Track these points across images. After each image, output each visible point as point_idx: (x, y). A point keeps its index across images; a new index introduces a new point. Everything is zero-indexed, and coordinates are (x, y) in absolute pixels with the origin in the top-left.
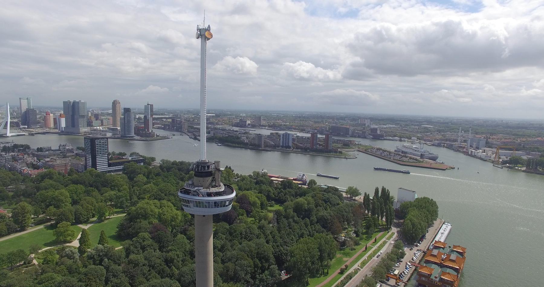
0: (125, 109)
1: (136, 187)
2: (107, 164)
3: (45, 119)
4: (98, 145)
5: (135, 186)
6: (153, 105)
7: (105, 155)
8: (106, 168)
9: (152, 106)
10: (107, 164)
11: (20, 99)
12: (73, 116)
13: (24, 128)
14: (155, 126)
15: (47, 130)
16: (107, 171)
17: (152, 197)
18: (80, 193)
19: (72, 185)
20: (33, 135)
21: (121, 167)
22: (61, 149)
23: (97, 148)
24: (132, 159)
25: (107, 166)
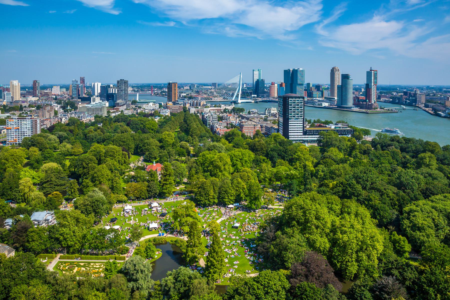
1: (322, 166)
2: (302, 131)
4: (291, 105)
5: (322, 164)
8: (300, 136)
11: (253, 70)
13: (254, 97)
14: (382, 99)
15: (271, 99)
16: (301, 140)
17: (340, 186)
18: (246, 162)
20: (257, 102)
21: (315, 138)
23: (291, 110)
25: (302, 134)
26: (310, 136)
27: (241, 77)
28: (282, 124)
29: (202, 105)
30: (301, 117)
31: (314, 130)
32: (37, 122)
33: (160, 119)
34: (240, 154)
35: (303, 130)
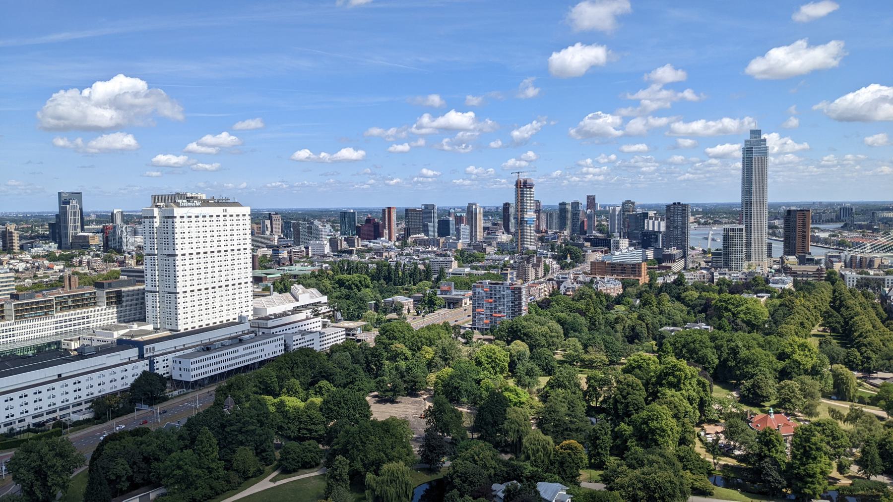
29: (876, 266)
32: (521, 293)
33: (771, 298)
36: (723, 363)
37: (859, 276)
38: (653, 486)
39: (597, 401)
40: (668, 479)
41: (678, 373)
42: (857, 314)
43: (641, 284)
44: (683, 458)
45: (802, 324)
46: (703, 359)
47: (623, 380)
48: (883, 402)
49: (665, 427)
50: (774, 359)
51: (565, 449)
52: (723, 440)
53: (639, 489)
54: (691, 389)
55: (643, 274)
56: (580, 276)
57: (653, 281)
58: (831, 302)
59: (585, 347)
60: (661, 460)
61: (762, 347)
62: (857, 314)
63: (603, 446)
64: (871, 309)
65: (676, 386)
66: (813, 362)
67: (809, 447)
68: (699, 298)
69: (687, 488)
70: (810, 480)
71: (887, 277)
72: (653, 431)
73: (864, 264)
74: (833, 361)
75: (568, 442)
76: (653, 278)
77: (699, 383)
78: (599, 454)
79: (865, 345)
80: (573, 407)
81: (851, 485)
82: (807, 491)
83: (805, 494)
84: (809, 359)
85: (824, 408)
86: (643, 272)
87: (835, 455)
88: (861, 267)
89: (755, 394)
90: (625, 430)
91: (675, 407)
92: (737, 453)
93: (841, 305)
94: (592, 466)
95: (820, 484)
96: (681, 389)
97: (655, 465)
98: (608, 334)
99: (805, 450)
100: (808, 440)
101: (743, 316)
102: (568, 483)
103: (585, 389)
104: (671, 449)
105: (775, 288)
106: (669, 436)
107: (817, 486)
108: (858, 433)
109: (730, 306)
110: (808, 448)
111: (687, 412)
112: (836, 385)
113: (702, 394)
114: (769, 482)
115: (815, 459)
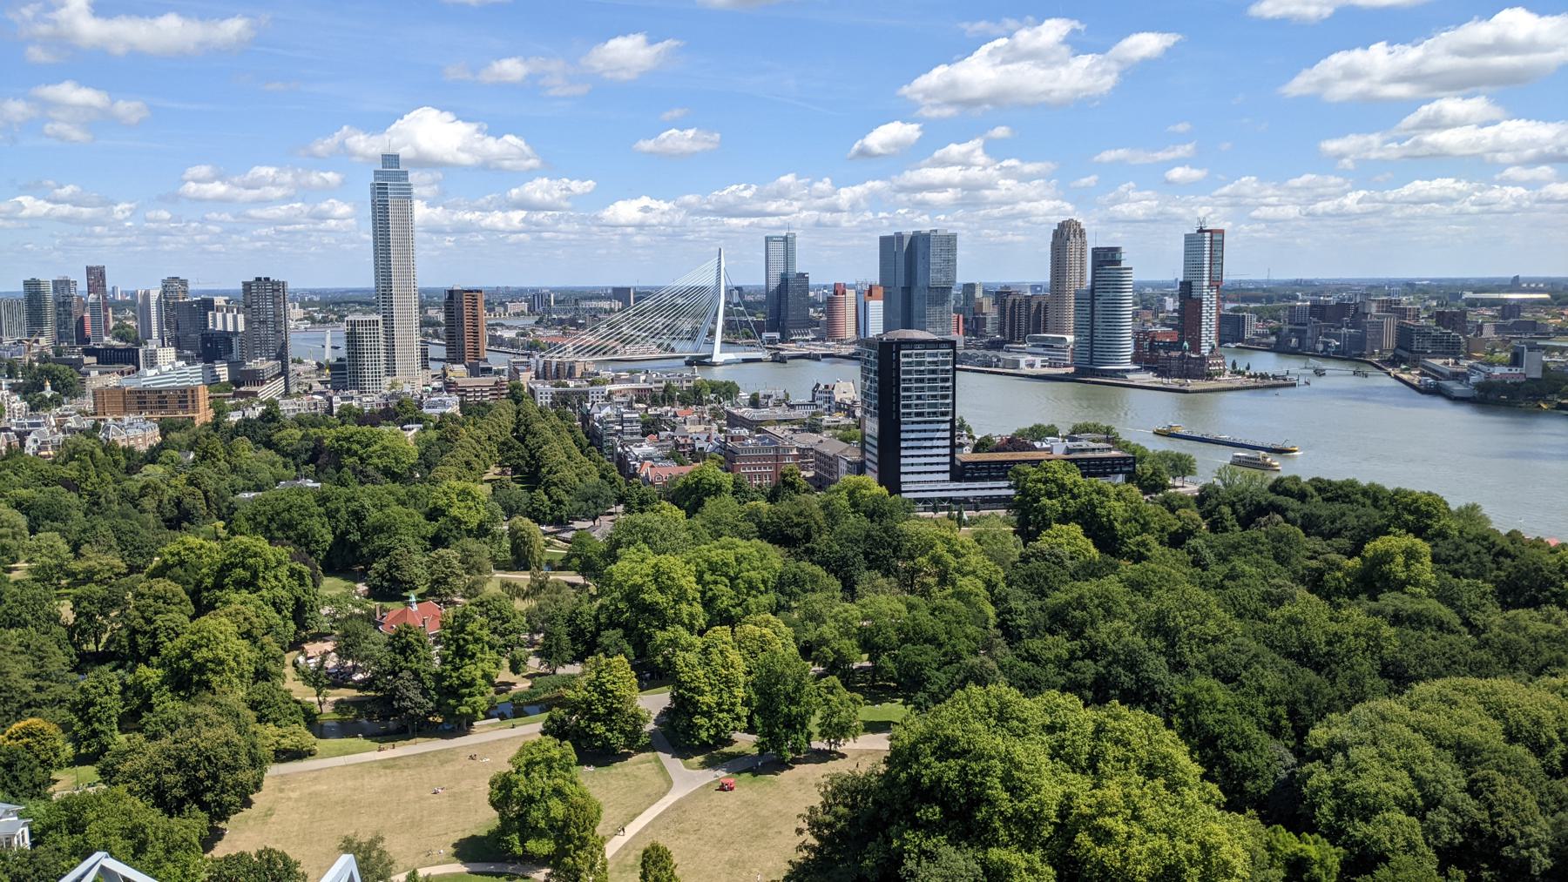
0: (1096, 252)
2: (947, 468)
3: (830, 305)
4: (909, 372)
6: (1222, 232)
7: (938, 422)
8: (939, 486)
9: (1217, 237)
10: (947, 468)
12: (908, 290)
13: (772, 341)
16: (944, 499)
19: (756, 541)
20: (783, 360)
21: (1002, 489)
22: (818, 402)
24: (1069, 451)
25: (947, 477)
26: (977, 485)
27: (723, 266)
28: (875, 443)
29: (578, 374)
30: (943, 414)
31: (989, 463)
33: (424, 430)
34: (732, 560)
35: (952, 463)
36: (341, 539)
37: (554, 390)
38: (193, 758)
39: (97, 644)
40: (223, 739)
41: (251, 561)
42: (546, 442)
43: (198, 425)
44: (260, 703)
45: (468, 463)
46: (306, 537)
47: (146, 591)
48: (576, 561)
49: (222, 655)
50: (419, 518)
51: (17, 739)
52: (332, 663)
53: (168, 771)
54: (279, 587)
55: (201, 408)
56: (70, 419)
57: (221, 417)
58: (515, 430)
59: (76, 548)
60: (210, 710)
61: (403, 504)
62: (546, 442)
63: (104, 717)
64: (565, 434)
65: (251, 585)
66: (480, 517)
67: (464, 639)
68: (304, 437)
69: (266, 751)
70: (467, 691)
71: (591, 389)
72: (200, 668)
73: (561, 371)
74: (510, 512)
75: (22, 724)
76: (220, 412)
77: (292, 573)
78: (95, 734)
79: (555, 484)
80: (41, 659)
81: (531, 687)
82: (464, 709)
83: (462, 715)
84: (473, 512)
85: (493, 583)
86: (201, 403)
87: (506, 646)
88: (558, 377)
89: (393, 580)
90: (147, 678)
91: (245, 619)
92: (358, 677)
93: (527, 431)
94: (79, 760)
95: (482, 694)
96: (259, 589)
97: (200, 722)
98: (125, 516)
99: (459, 647)
100: (462, 629)
101: (376, 461)
102: (25, 800)
103: (71, 621)
104: (237, 695)
105: (430, 415)
106: (232, 670)
107: (478, 698)
108: (540, 609)
109: (355, 447)
110: (461, 642)
111: (271, 627)
112: (515, 549)
113: (299, 591)
114: (406, 709)
115: (473, 656)
